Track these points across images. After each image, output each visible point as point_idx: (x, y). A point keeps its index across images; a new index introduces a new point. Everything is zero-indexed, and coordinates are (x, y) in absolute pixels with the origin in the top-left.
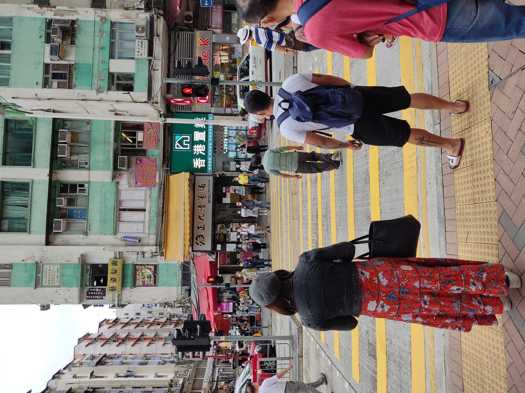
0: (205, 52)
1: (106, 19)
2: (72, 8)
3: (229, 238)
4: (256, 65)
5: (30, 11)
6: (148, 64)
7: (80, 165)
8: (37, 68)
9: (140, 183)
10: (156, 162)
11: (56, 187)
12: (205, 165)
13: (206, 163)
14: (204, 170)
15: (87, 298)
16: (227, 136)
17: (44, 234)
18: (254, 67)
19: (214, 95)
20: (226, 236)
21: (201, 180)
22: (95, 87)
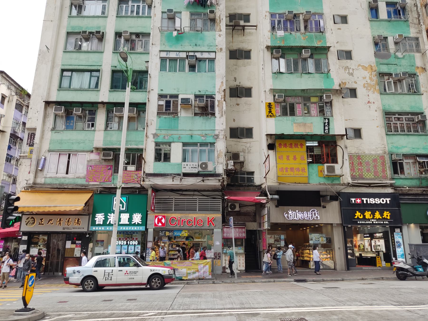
0: (202, 222)
1: (216, 138)
2: (225, 113)
3: (34, 247)
4: (128, 274)
5: (220, 83)
6: (174, 173)
7: (110, 123)
8: (175, 89)
9: (90, 169)
10: (108, 182)
11: (93, 107)
12: (98, 224)
13: (99, 225)
14: (94, 223)
15: (29, 133)
16: (129, 244)
17: (56, 100)
18: (127, 272)
19: (166, 231)
20: (36, 244)
21: (84, 220)
22: (159, 132)
